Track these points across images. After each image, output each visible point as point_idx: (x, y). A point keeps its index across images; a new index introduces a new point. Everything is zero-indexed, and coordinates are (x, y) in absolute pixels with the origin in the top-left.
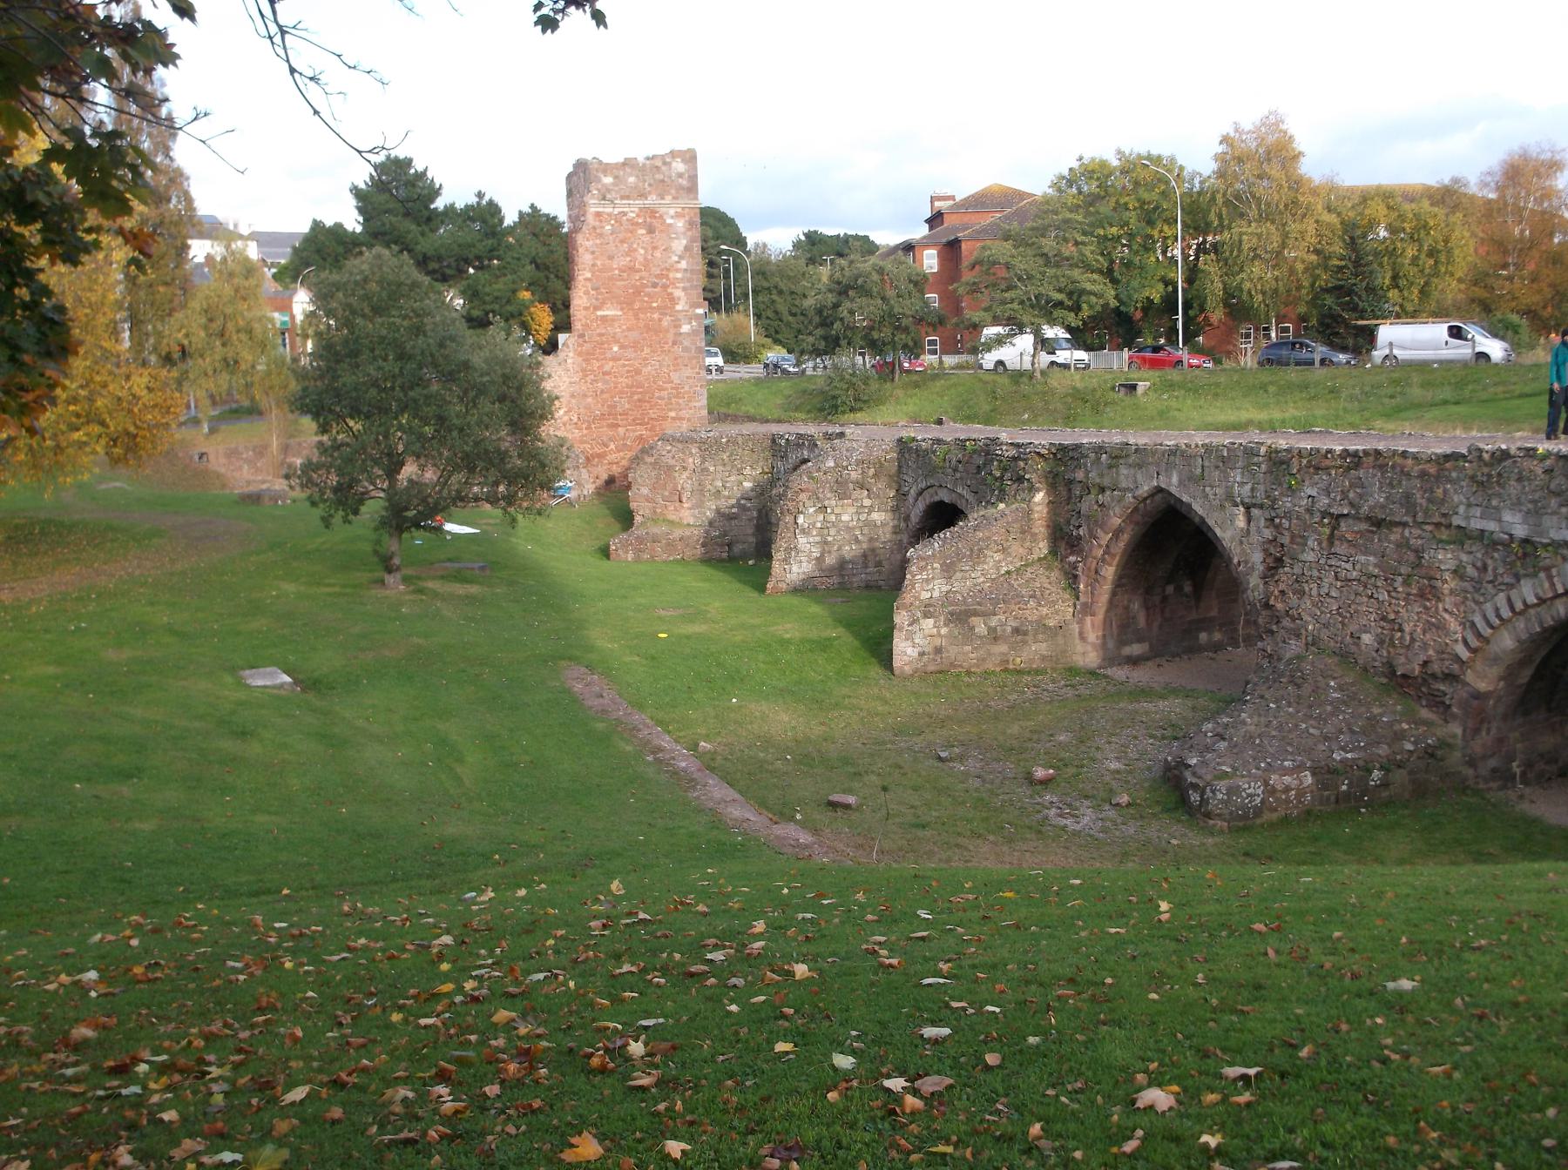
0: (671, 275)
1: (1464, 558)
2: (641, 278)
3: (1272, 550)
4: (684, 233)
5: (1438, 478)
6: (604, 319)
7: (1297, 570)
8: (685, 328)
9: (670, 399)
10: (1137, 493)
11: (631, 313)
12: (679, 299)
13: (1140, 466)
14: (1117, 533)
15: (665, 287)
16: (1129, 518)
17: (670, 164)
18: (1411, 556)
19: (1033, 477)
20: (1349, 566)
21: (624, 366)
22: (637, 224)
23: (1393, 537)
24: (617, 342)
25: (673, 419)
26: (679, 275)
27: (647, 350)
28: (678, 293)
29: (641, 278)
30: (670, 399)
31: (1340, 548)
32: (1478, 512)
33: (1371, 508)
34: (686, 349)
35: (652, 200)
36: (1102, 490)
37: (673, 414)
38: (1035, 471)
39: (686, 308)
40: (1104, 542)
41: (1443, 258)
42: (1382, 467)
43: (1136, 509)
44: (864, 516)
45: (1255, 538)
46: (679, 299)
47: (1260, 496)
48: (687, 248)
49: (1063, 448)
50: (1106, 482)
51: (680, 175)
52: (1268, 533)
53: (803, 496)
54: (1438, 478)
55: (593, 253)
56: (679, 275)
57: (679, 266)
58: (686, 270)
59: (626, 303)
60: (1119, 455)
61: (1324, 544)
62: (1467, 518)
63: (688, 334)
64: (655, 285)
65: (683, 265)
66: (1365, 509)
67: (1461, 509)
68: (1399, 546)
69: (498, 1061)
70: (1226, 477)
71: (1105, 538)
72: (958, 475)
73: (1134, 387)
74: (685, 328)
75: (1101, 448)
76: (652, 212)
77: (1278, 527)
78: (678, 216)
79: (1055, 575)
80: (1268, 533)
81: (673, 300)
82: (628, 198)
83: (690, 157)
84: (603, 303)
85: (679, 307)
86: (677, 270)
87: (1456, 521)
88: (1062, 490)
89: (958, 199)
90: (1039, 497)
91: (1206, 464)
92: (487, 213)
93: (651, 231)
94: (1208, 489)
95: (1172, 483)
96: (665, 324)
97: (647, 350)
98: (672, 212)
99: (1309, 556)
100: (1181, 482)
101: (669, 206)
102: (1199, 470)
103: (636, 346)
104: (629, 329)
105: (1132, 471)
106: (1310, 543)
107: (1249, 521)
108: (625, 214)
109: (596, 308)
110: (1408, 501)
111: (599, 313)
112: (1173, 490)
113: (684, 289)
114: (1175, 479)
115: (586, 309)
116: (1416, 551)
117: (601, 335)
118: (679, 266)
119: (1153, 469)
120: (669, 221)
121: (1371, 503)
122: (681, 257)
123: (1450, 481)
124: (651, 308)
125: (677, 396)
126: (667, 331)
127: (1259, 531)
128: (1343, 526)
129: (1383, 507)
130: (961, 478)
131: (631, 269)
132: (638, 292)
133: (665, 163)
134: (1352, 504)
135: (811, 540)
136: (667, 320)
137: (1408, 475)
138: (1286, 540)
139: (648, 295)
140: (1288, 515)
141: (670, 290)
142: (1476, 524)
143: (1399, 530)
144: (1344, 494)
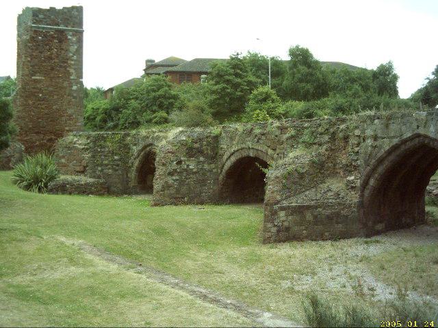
6: (35, 80)
15: (65, 67)
22: (54, 38)
24: (42, 93)
26: (73, 62)
28: (72, 71)
34: (74, 98)
37: (67, 128)
44: (200, 167)
48: (77, 50)
55: (32, 49)
56: (73, 62)
59: (46, 75)
63: (76, 91)
64: (61, 66)
76: (62, 32)
78: (73, 35)
81: (70, 74)
83: (81, 8)
85: (72, 78)
86: (72, 60)
89: (156, 62)
93: (60, 41)
104: (47, 87)
108: (49, 32)
109: (35, 76)
111: (33, 78)
113: (75, 69)
122: (74, 55)
124: (59, 77)
131: (50, 58)
132: (52, 69)
133: (69, 11)
135: (174, 178)
139: (58, 71)
141: (68, 69)
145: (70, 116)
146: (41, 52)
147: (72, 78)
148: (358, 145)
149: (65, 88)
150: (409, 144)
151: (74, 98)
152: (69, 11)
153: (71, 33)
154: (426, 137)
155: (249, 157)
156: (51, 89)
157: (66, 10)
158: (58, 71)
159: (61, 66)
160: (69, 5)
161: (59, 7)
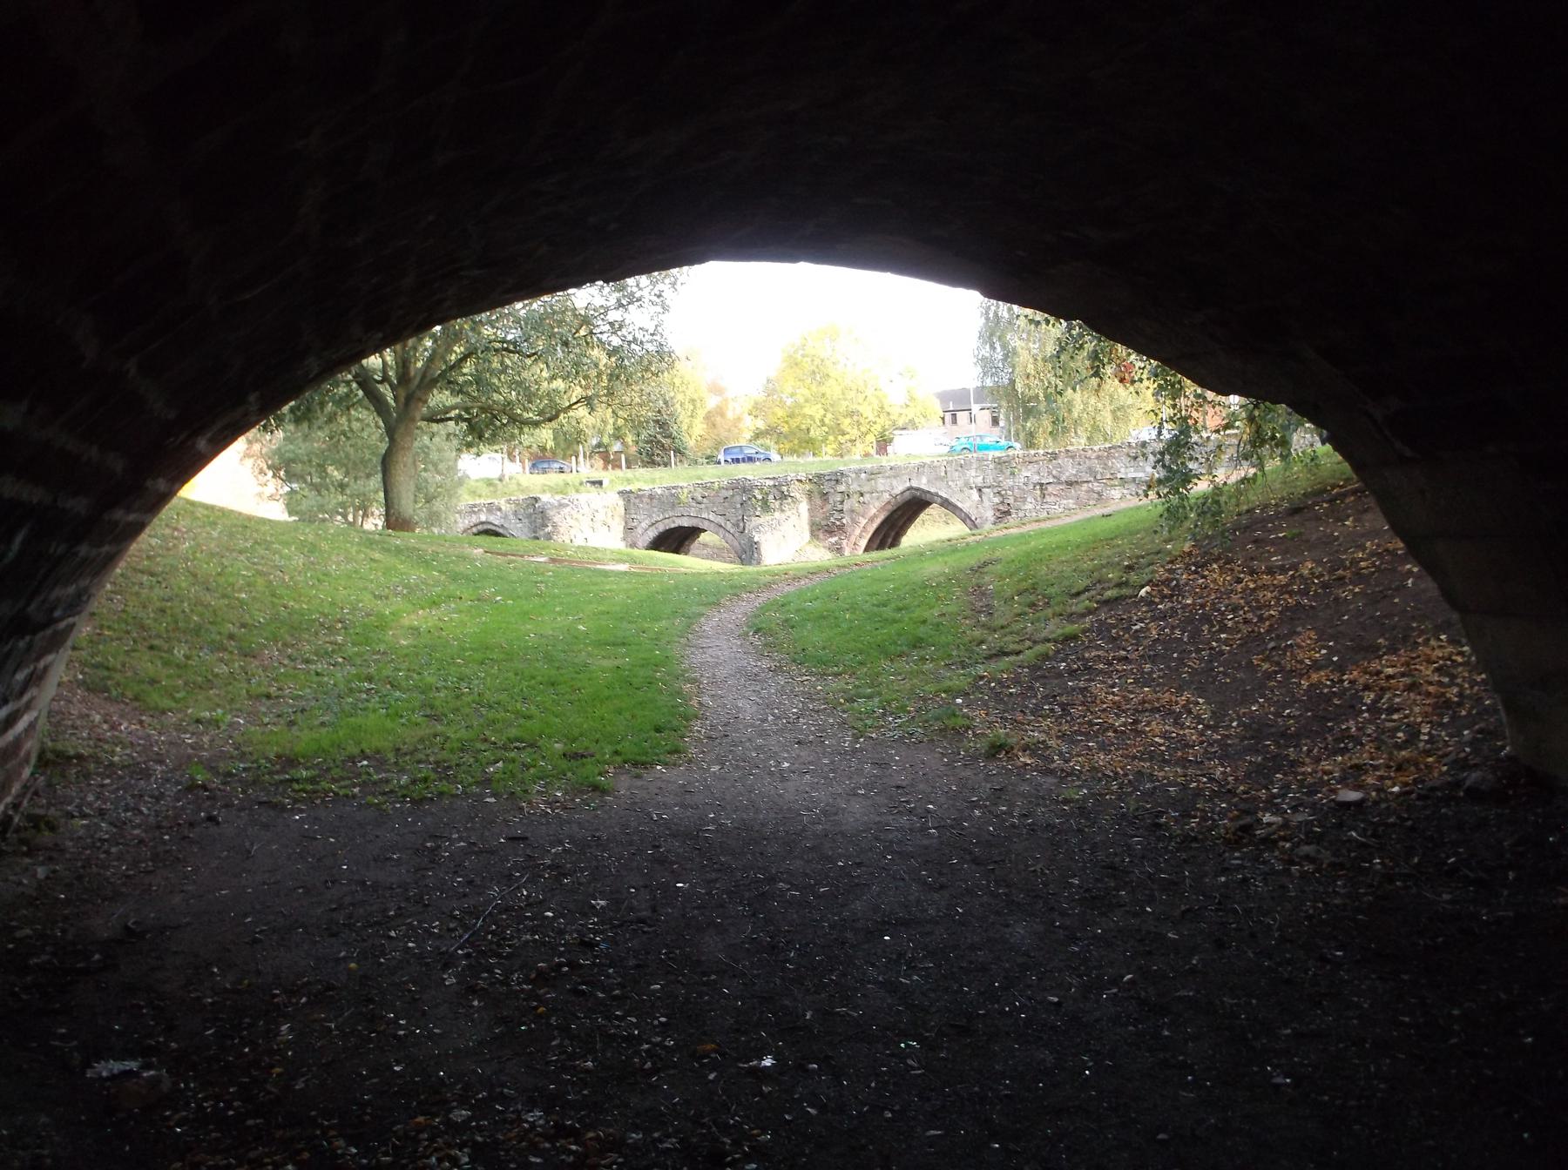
1: (1125, 491)
3: (1001, 508)
5: (1108, 457)
7: (1021, 514)
10: (892, 492)
13: (895, 477)
14: (872, 520)
16: (883, 508)
18: (1096, 496)
19: (798, 496)
20: (1056, 507)
23: (1083, 489)
31: (1048, 499)
32: (1132, 469)
33: (1068, 477)
36: (862, 495)
38: (797, 491)
40: (862, 525)
41: (698, 405)
42: (1073, 457)
43: (889, 502)
45: (987, 503)
47: (990, 481)
49: (819, 476)
50: (865, 489)
52: (997, 500)
53: (573, 532)
54: (1108, 457)
60: (873, 474)
61: (1039, 499)
62: (1126, 473)
66: (1063, 478)
67: (1123, 470)
68: (1087, 492)
69: (1154, 602)
70: (964, 474)
71: (863, 521)
72: (703, 506)
73: (600, 483)
75: (860, 470)
77: (1002, 496)
79: (823, 550)
80: (997, 500)
87: (1119, 476)
88: (819, 502)
90: (804, 507)
91: (948, 469)
94: (950, 483)
95: (923, 483)
99: (1029, 506)
100: (928, 481)
102: (943, 474)
105: (888, 480)
106: (1029, 500)
107: (980, 496)
110: (1091, 470)
112: (923, 487)
114: (924, 480)
116: (1098, 493)
119: (906, 478)
121: (1067, 474)
123: (1114, 458)
127: (990, 500)
128: (1050, 488)
129: (1075, 475)
130: (707, 507)
134: (1054, 477)
137: (1090, 458)
138: (1011, 501)
140: (1012, 489)
142: (1131, 475)
143: (1086, 485)
144: (1050, 473)
148: (842, 502)
154: (918, 489)
155: (680, 528)
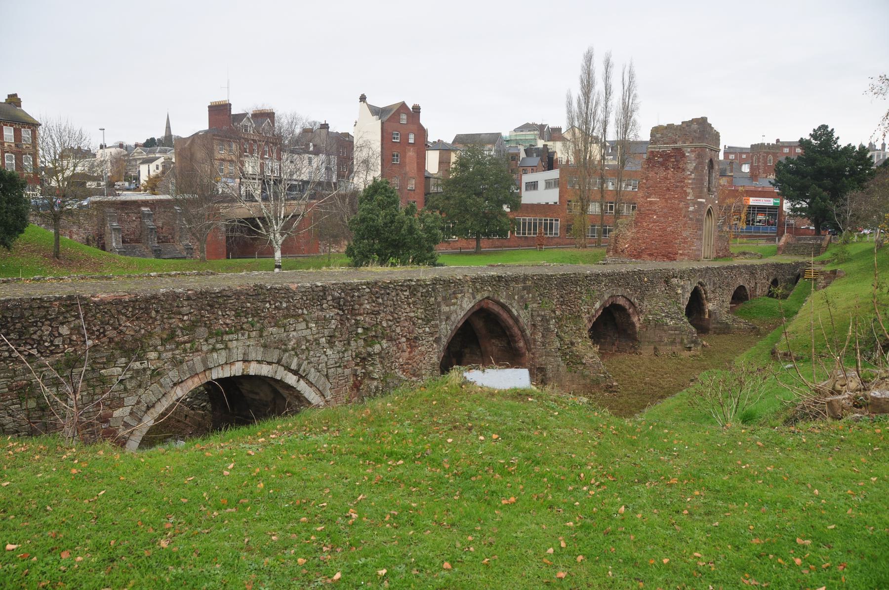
0: (686, 181)
2: (670, 183)
4: (695, 160)
6: (651, 203)
8: (691, 209)
9: (680, 244)
11: (664, 200)
12: (689, 193)
15: (682, 187)
17: (690, 126)
21: (659, 226)
25: (681, 254)
26: (690, 181)
27: (670, 219)
28: (689, 190)
29: (670, 183)
30: (680, 244)
34: (691, 219)
35: (679, 145)
37: (681, 252)
39: (693, 198)
46: (689, 193)
48: (695, 168)
51: (695, 131)
56: (690, 181)
57: (690, 177)
58: (694, 179)
63: (693, 212)
64: (677, 187)
65: (693, 176)
74: (691, 209)
78: (692, 151)
81: (687, 194)
82: (667, 144)
84: (651, 194)
85: (688, 198)
86: (689, 179)
92: (768, 144)
96: (681, 206)
97: (670, 219)
98: (689, 150)
101: (687, 147)
103: (665, 216)
104: (662, 208)
109: (650, 198)
113: (692, 188)
115: (642, 197)
117: (648, 210)
118: (690, 177)
120: (687, 154)
122: (692, 172)
125: (685, 242)
126: (681, 209)
136: (682, 205)
145: (686, 238)
146: (657, 174)
147: (688, 198)
149: (681, 209)
150: (505, 315)
151: (691, 219)
152: (687, 126)
153: (689, 150)
156: (665, 210)
157: (684, 126)
158: (674, 191)
159: (677, 187)
160: (688, 119)
161: (678, 122)
